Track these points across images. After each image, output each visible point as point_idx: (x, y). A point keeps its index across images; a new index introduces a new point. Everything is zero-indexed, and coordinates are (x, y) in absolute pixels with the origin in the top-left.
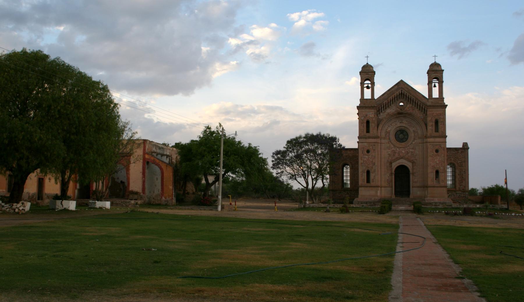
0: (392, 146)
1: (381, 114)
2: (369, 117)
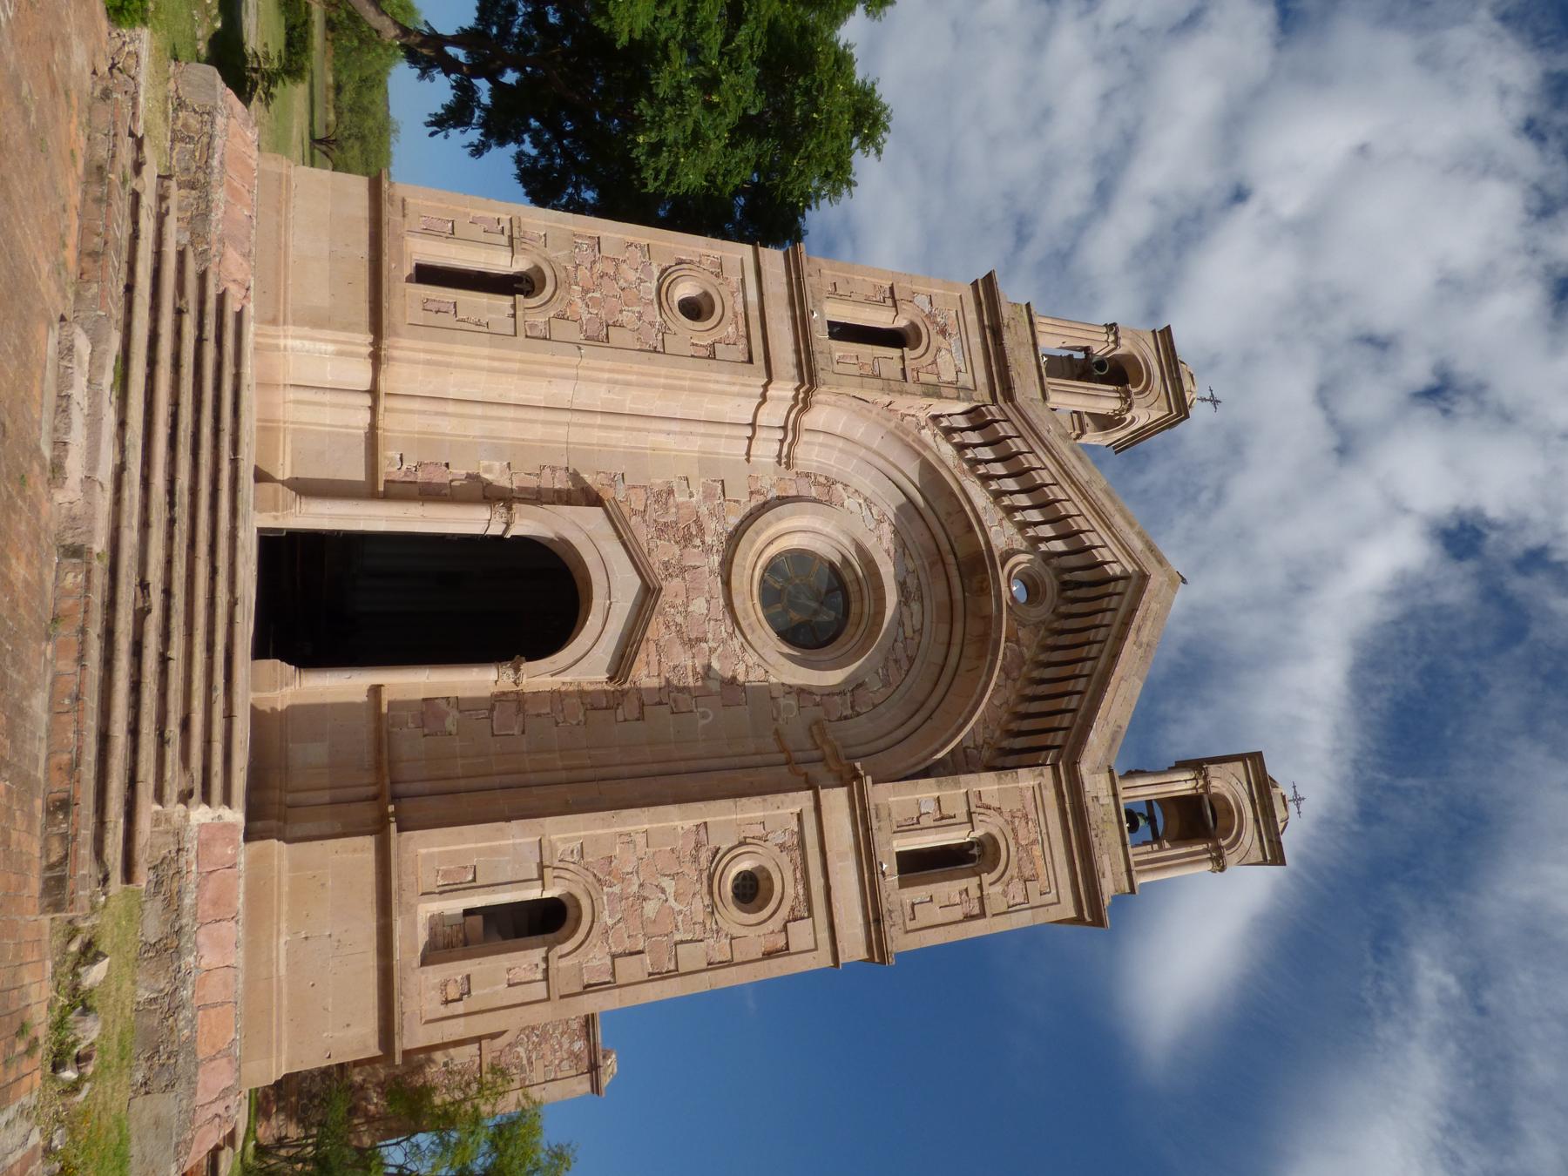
0: (733, 521)
1: (947, 451)
2: (939, 350)
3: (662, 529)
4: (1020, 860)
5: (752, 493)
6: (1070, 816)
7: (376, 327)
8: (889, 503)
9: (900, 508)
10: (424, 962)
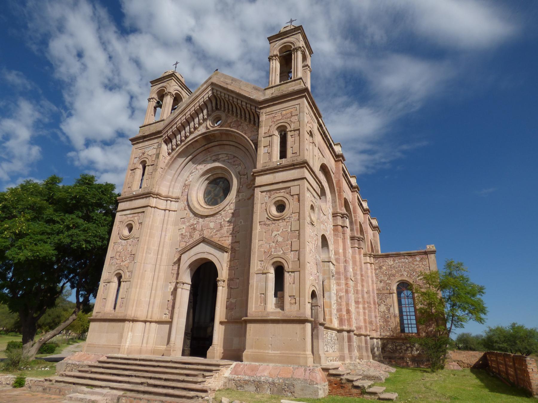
0: (191, 215)
1: (177, 149)
3: (191, 237)
4: (286, 118)
5: (185, 210)
6: (275, 103)
7: (123, 320)
8: (191, 166)
9: (193, 163)
10: (282, 308)
